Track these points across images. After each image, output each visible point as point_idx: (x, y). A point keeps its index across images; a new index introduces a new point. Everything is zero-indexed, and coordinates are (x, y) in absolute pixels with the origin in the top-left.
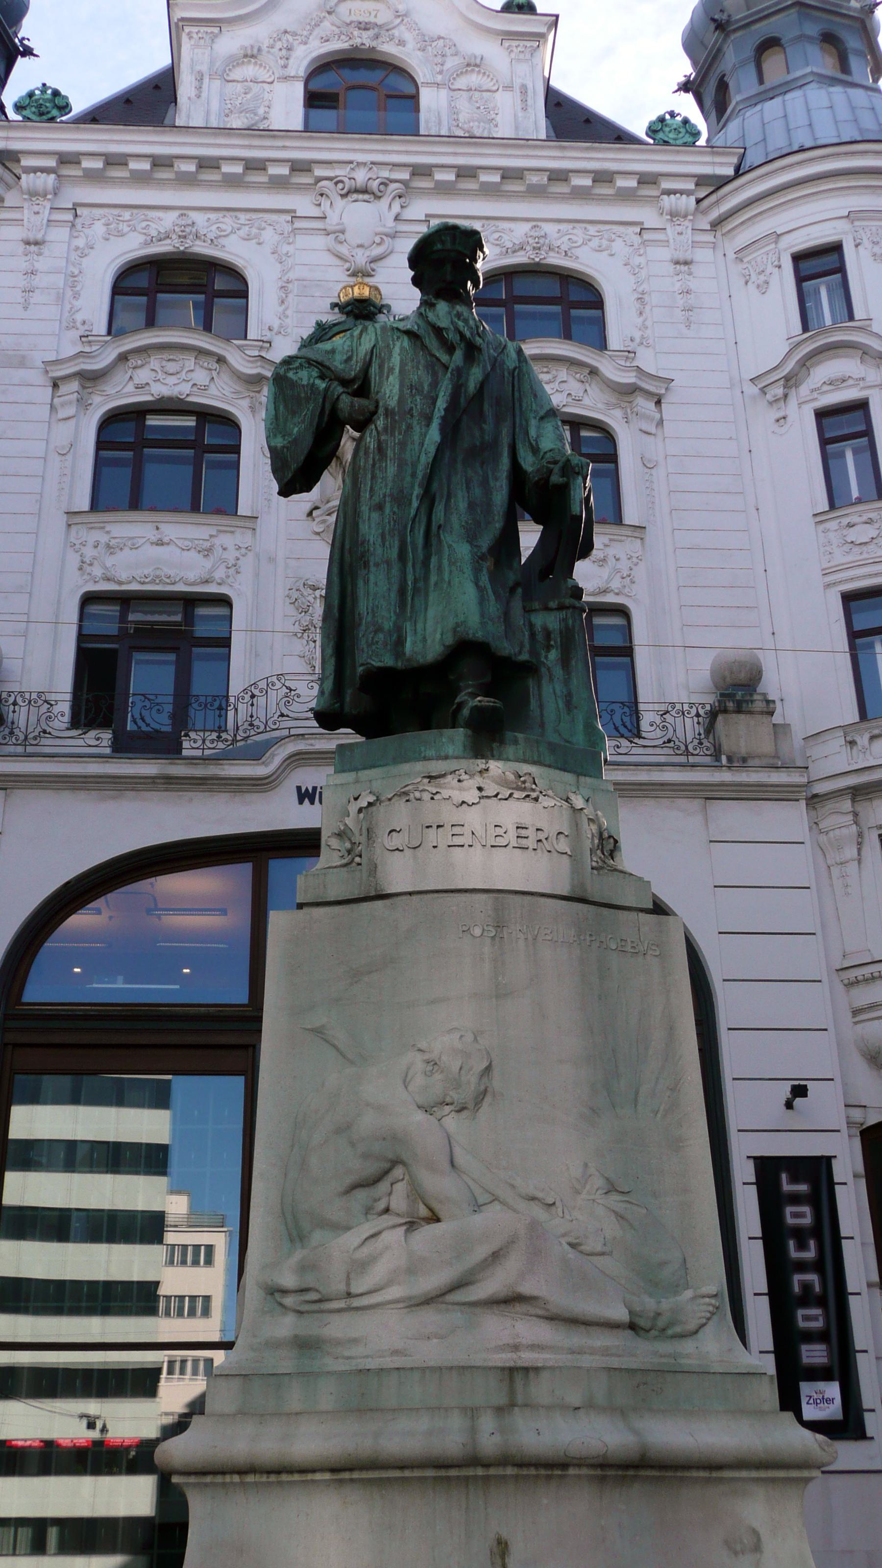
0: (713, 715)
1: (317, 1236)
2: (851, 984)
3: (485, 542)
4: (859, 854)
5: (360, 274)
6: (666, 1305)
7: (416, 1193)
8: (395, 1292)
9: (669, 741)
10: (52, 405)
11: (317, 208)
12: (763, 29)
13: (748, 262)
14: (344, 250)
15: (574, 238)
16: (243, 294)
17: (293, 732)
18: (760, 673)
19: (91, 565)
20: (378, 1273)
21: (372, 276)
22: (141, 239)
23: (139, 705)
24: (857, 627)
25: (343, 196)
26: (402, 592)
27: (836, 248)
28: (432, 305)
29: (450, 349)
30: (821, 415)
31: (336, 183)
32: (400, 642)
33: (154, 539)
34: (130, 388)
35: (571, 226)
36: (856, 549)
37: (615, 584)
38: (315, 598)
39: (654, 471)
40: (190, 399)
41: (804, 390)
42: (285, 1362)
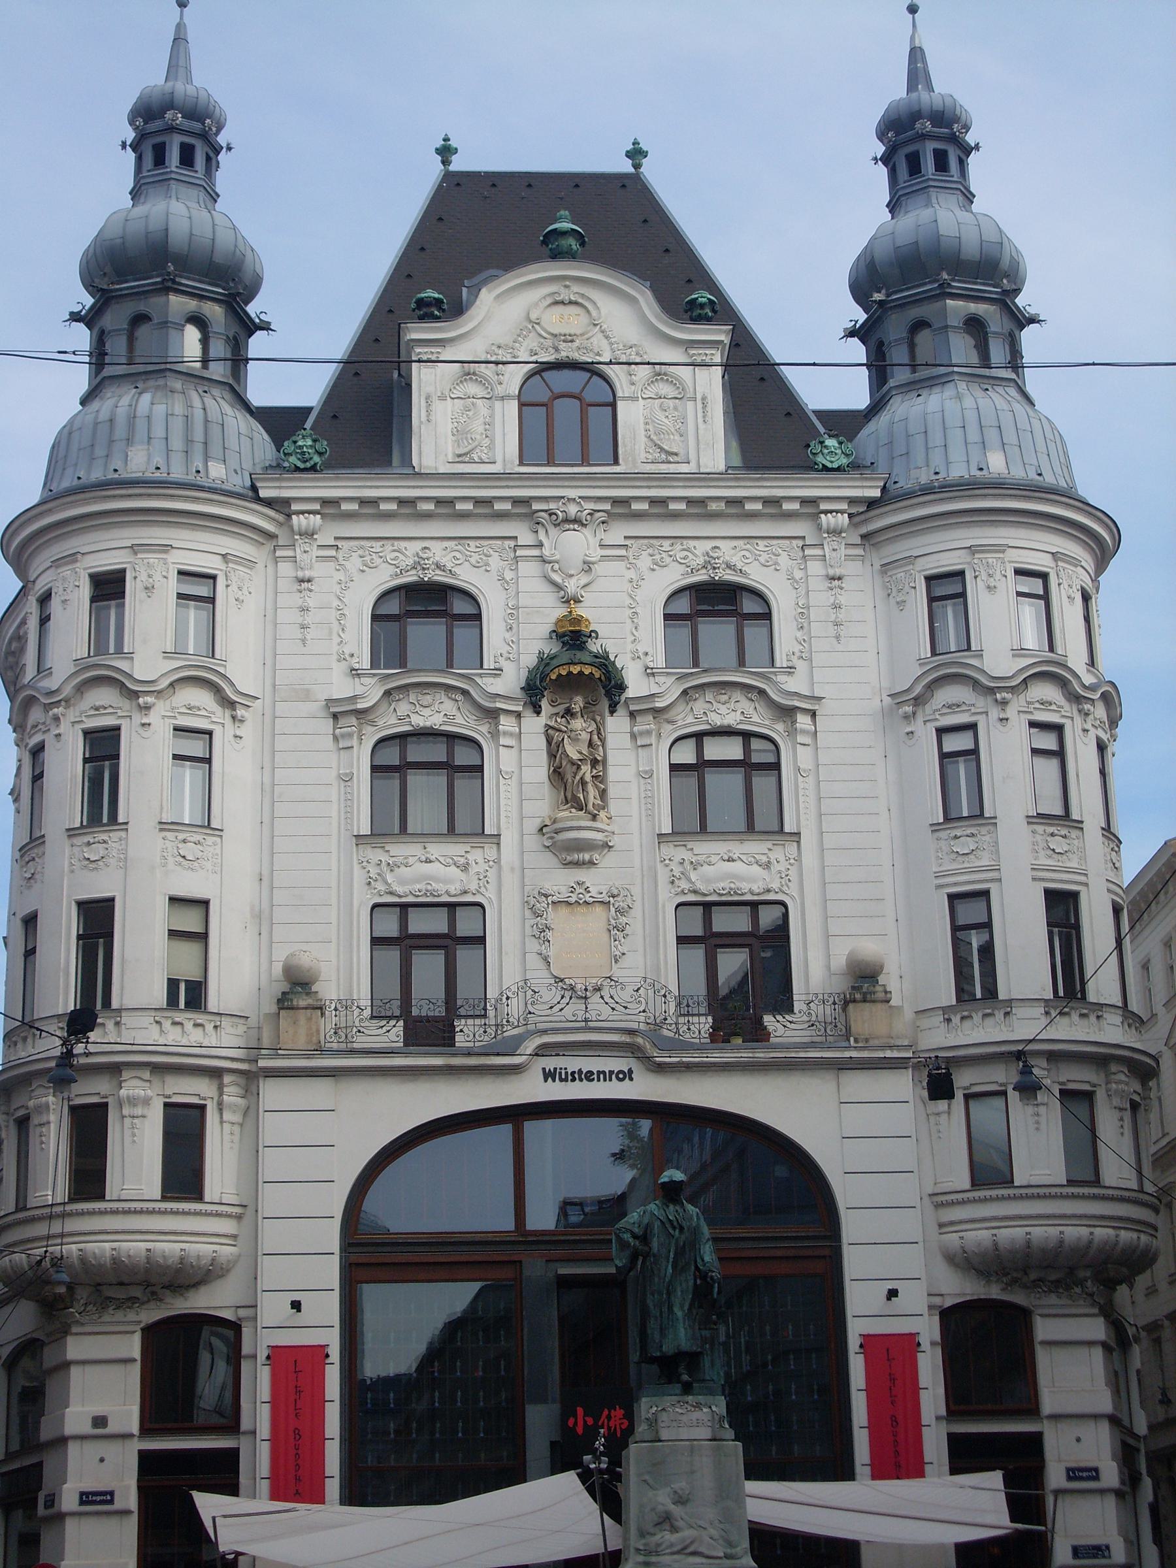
0: (846, 1003)
1: (648, 1536)
2: (939, 1206)
3: (686, 1307)
4: (949, 1108)
5: (572, 602)
6: (733, 1551)
7: (672, 1526)
8: (668, 1551)
9: (813, 1025)
11: (535, 534)
12: (915, 313)
13: (891, 576)
14: (557, 578)
15: (747, 554)
16: (478, 617)
17: (541, 1026)
18: (882, 967)
20: (664, 1546)
21: (581, 601)
22: (392, 570)
24: (961, 922)
25: (556, 525)
26: (661, 1329)
27: (961, 574)
28: (668, 1206)
29: (674, 1228)
30: (941, 731)
32: (661, 1346)
33: (423, 859)
34: (393, 721)
36: (960, 859)
37: (775, 885)
38: (548, 904)
39: (806, 779)
40: (443, 728)
41: (928, 708)
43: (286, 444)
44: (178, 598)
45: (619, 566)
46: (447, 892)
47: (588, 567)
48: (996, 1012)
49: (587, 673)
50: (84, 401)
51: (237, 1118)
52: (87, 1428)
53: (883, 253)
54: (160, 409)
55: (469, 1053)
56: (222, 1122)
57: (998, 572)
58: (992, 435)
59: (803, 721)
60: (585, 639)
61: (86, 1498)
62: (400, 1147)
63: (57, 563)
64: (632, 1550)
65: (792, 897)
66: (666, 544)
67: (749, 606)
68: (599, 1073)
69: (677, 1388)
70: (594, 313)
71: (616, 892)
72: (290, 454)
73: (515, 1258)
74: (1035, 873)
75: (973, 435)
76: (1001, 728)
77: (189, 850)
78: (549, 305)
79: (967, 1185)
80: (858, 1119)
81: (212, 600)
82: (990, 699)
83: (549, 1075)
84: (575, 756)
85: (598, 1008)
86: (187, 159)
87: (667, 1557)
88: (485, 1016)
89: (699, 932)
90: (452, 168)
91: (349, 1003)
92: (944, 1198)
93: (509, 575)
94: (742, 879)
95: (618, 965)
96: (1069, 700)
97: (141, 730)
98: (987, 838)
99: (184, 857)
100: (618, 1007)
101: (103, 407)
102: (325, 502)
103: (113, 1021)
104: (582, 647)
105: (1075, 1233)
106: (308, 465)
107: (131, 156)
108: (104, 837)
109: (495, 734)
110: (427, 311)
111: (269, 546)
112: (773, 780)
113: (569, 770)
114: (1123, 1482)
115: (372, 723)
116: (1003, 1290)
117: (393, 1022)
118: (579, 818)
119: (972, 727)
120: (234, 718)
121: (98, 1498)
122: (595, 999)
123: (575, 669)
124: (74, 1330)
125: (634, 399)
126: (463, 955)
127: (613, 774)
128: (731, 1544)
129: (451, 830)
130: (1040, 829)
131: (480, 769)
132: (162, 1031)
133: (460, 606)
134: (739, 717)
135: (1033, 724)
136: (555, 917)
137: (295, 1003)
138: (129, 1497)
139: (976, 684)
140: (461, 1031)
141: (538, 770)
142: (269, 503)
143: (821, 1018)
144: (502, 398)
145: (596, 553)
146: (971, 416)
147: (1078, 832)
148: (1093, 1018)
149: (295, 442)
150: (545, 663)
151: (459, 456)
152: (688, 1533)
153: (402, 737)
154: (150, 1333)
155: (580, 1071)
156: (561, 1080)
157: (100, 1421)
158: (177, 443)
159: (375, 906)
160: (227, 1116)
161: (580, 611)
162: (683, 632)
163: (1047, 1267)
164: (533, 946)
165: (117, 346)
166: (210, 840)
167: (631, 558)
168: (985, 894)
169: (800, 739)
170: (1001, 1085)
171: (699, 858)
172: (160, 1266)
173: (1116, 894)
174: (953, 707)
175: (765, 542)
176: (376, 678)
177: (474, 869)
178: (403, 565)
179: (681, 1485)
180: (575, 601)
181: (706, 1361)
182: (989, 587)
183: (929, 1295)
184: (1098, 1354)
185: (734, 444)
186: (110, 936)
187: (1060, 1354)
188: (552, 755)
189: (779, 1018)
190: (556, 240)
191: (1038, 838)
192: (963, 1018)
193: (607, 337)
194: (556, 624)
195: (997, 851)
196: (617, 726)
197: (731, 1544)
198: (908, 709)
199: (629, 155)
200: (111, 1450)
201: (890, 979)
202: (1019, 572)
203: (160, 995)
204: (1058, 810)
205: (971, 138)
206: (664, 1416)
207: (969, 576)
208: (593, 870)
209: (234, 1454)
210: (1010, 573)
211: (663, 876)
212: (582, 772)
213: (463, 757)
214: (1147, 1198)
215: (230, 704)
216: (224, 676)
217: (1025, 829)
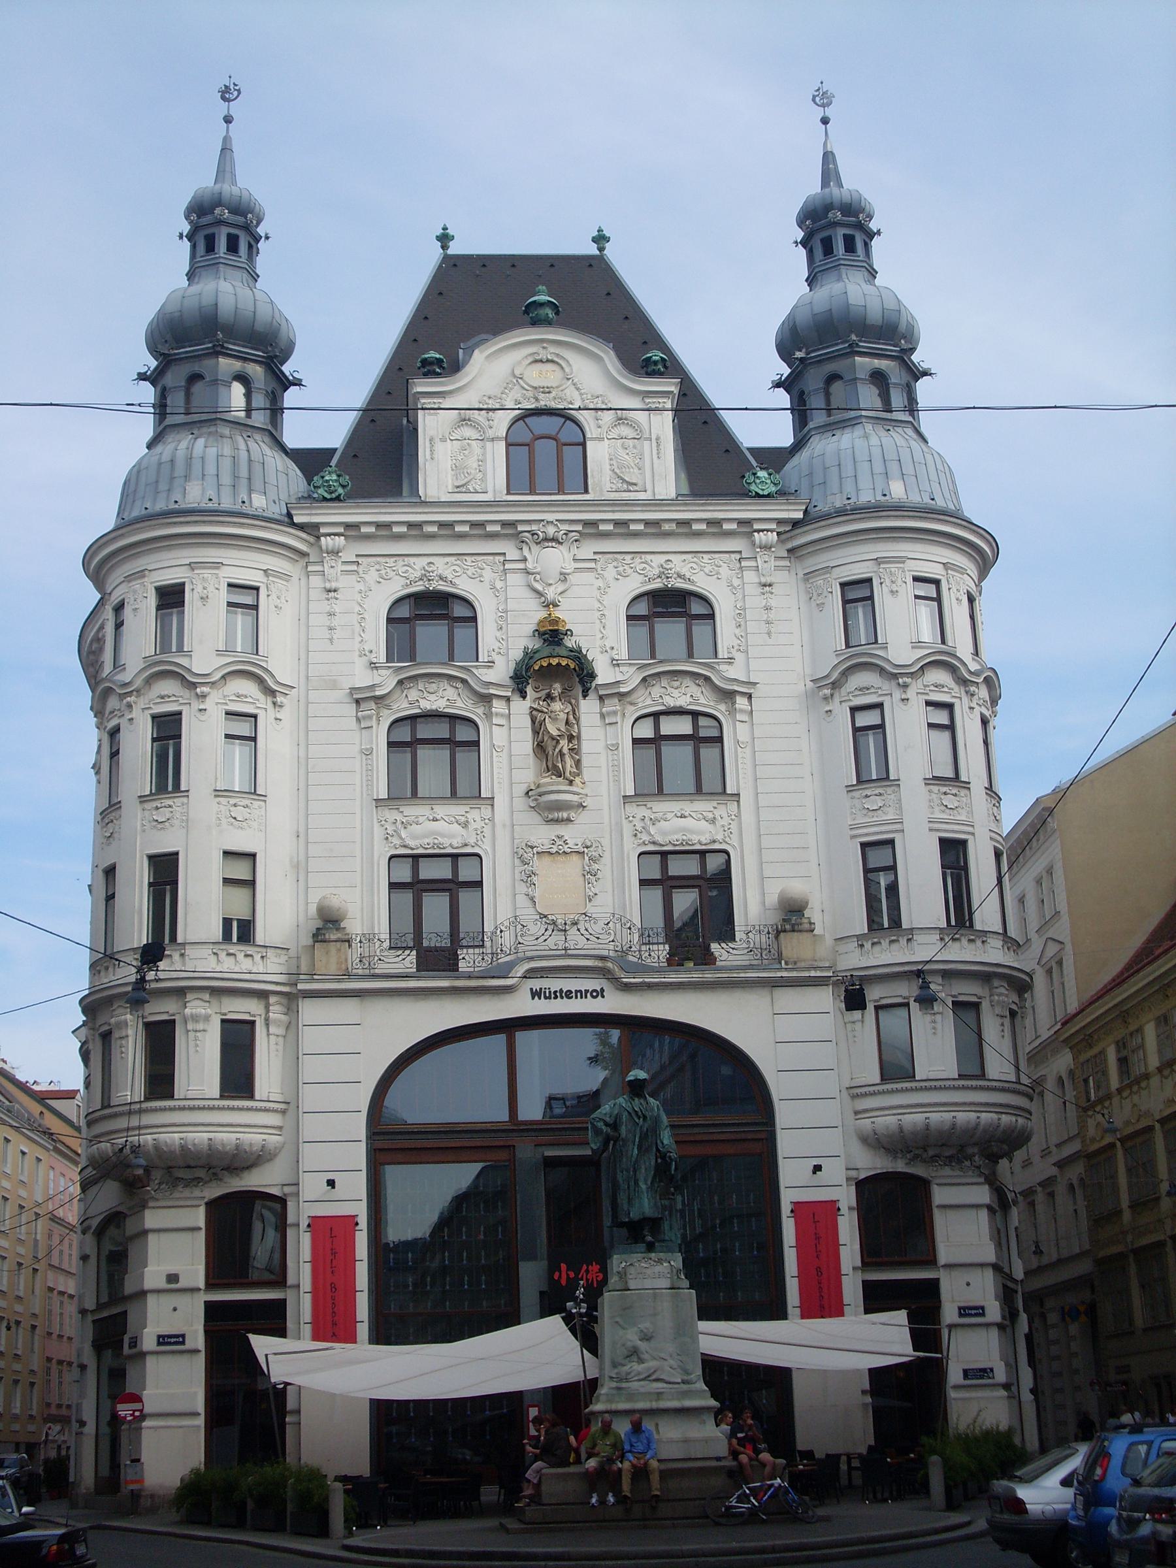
0: (778, 933)
3: (649, 1183)
10: (356, 717)
11: (519, 551)
14: (540, 588)
16: (474, 619)
17: (529, 954)
18: (807, 903)
19: (392, 836)
20: (633, 1374)
22: (403, 581)
23: (434, 940)
24: (871, 866)
25: (537, 543)
27: (869, 581)
29: (639, 1119)
30: (854, 710)
31: (533, 535)
34: (405, 705)
35: (693, 555)
36: (871, 814)
37: (719, 837)
41: (843, 691)
42: (614, 1392)
43: (315, 478)
44: (228, 606)
45: (589, 577)
46: (451, 845)
47: (564, 577)
48: (900, 939)
49: (564, 664)
50: (150, 446)
51: (281, 1031)
52: (162, 1284)
53: (803, 318)
54: (212, 452)
55: (470, 976)
56: (268, 1035)
57: (899, 580)
58: (893, 467)
59: (741, 702)
60: (562, 636)
61: (162, 1340)
62: (417, 1053)
63: (129, 578)
64: (607, 1379)
65: (734, 847)
66: (628, 557)
67: (696, 608)
68: (577, 991)
69: (642, 1247)
70: (567, 370)
71: (589, 844)
72: (318, 487)
73: (510, 1143)
74: (931, 825)
75: (878, 467)
76: (904, 707)
77: (239, 812)
78: (530, 363)
79: (877, 1080)
80: (789, 1027)
81: (255, 607)
82: (894, 683)
83: (535, 994)
84: (555, 733)
85: (575, 939)
86: (233, 247)
87: (636, 1383)
88: (482, 946)
89: (658, 876)
90: (450, 252)
91: (371, 937)
92: (859, 1091)
93: (499, 585)
94: (692, 832)
95: (591, 904)
96: (957, 683)
97: (198, 715)
98: (892, 796)
99: (235, 818)
100: (592, 938)
101: (165, 450)
102: (348, 526)
103: (178, 953)
104: (559, 643)
105: (964, 1117)
106: (334, 496)
107: (187, 244)
108: (170, 802)
109: (489, 715)
110: (430, 369)
111: (302, 562)
112: (717, 751)
113: (550, 745)
114: (1003, 1317)
115: (388, 707)
116: (907, 1164)
117: (407, 952)
118: (558, 784)
119: (879, 706)
120: (274, 703)
121: (173, 1340)
122: (573, 931)
123: (554, 661)
124: (151, 1204)
125: (601, 439)
126: (464, 896)
127: (586, 747)
128: (687, 1372)
129: (454, 794)
130: (935, 789)
131: (476, 744)
132: (218, 961)
133: (459, 611)
134: (689, 699)
135: (929, 703)
136: (538, 864)
137: (327, 936)
138: (197, 1338)
139: (882, 671)
140: (464, 958)
141: (525, 743)
142: (301, 527)
143: (758, 945)
144: (493, 440)
145: (570, 566)
146: (876, 452)
147: (966, 791)
148: (979, 943)
149: (323, 477)
150: (529, 656)
151: (458, 487)
152: (652, 1364)
153: (413, 718)
154: (213, 1206)
155: (561, 990)
156: (546, 998)
157: (173, 1278)
158: (226, 479)
159: (392, 857)
160: (272, 1030)
161: (558, 613)
162: (642, 630)
163: (943, 1145)
164: (522, 888)
165: (176, 400)
166: (256, 804)
167: (599, 569)
168: (891, 842)
169: (739, 717)
170: (905, 998)
171: (657, 815)
172: (219, 1152)
173: (998, 842)
174: (863, 690)
175: (709, 556)
176: (391, 670)
177: (472, 826)
178: (412, 577)
179: (646, 1325)
180: (554, 606)
181: (666, 1225)
182: (892, 591)
183: (847, 1169)
184: (984, 1214)
185: (683, 476)
186: (175, 883)
187: (952, 1215)
188: (536, 732)
189: (724, 945)
190: (536, 309)
191: (934, 796)
192: (873, 944)
193: (578, 389)
194: (538, 624)
195: (901, 808)
196: (588, 707)
197: (687, 1372)
198: (827, 692)
199: (595, 240)
200: (182, 1301)
201: (814, 913)
202: (916, 579)
203: (217, 932)
204: (950, 774)
205: (873, 225)
206: (632, 1270)
207: (875, 583)
208: (570, 826)
209: (282, 1303)
210: (910, 580)
211: (627, 830)
212: (561, 746)
213: (463, 734)
214: (1023, 1088)
215: (272, 693)
216: (266, 670)
217: (924, 790)
